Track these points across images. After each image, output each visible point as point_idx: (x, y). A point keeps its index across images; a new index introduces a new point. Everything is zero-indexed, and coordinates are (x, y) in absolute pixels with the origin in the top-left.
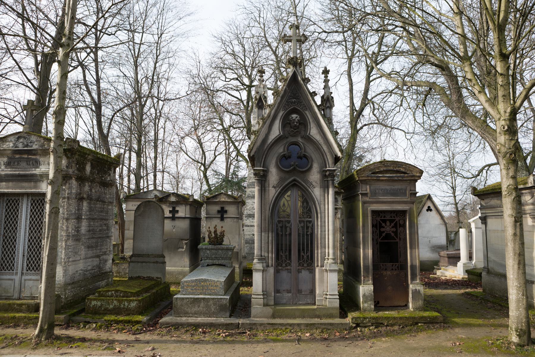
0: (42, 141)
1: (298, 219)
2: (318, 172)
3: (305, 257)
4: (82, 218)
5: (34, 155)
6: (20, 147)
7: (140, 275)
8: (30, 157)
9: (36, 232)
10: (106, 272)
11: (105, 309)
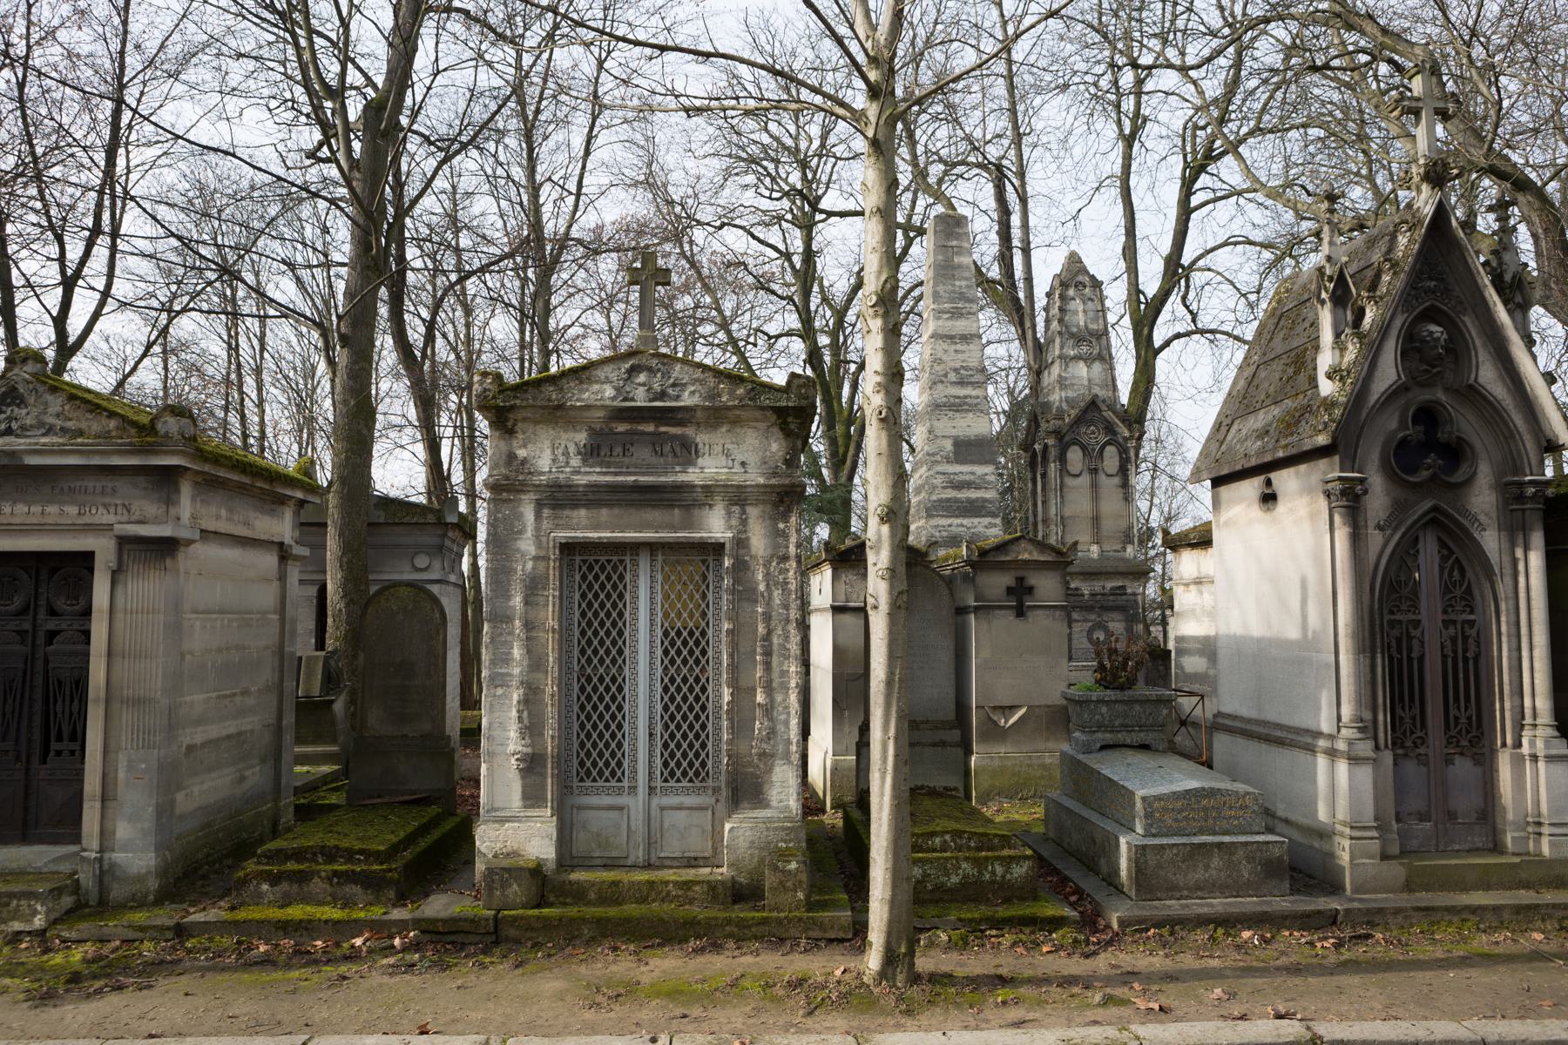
0: (712, 382)
1: (1440, 617)
2: (1491, 487)
3: (1463, 720)
5: (682, 423)
6: (640, 399)
8: (663, 429)
9: (685, 662)
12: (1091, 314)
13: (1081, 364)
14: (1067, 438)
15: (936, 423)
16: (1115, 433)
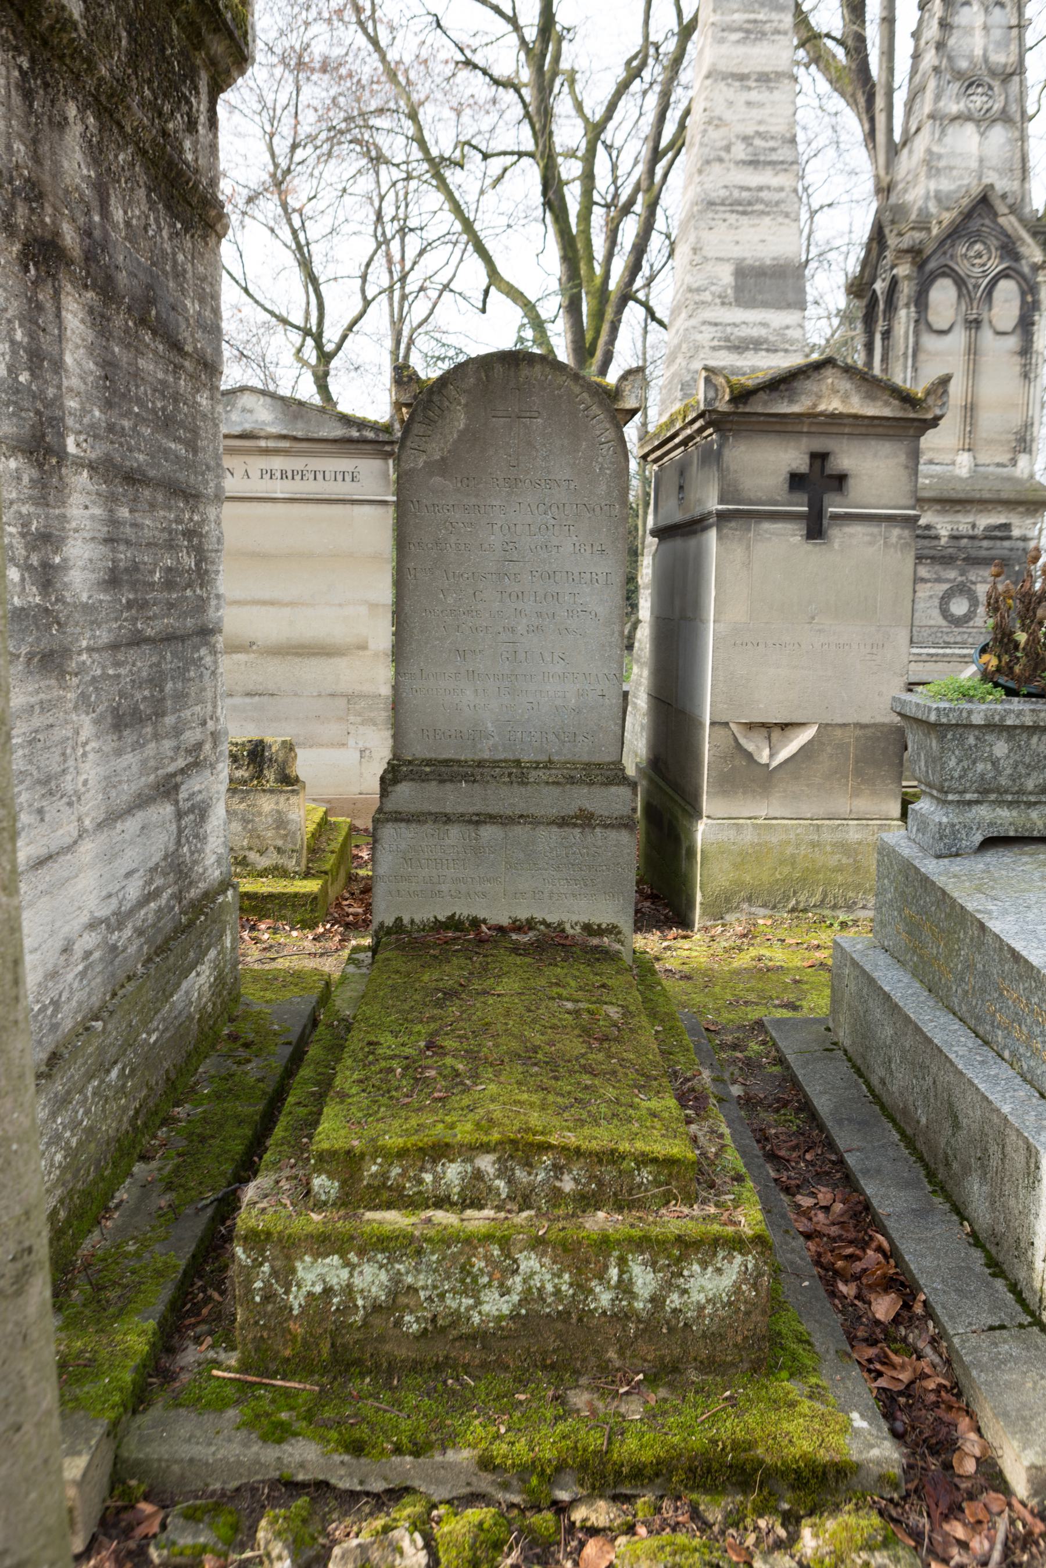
4: (62, 455)
7: (464, 910)
10: (206, 895)
11: (436, 1330)
12: (997, 34)
13: (970, 128)
14: (932, 265)
15: (706, 235)
16: (1016, 257)
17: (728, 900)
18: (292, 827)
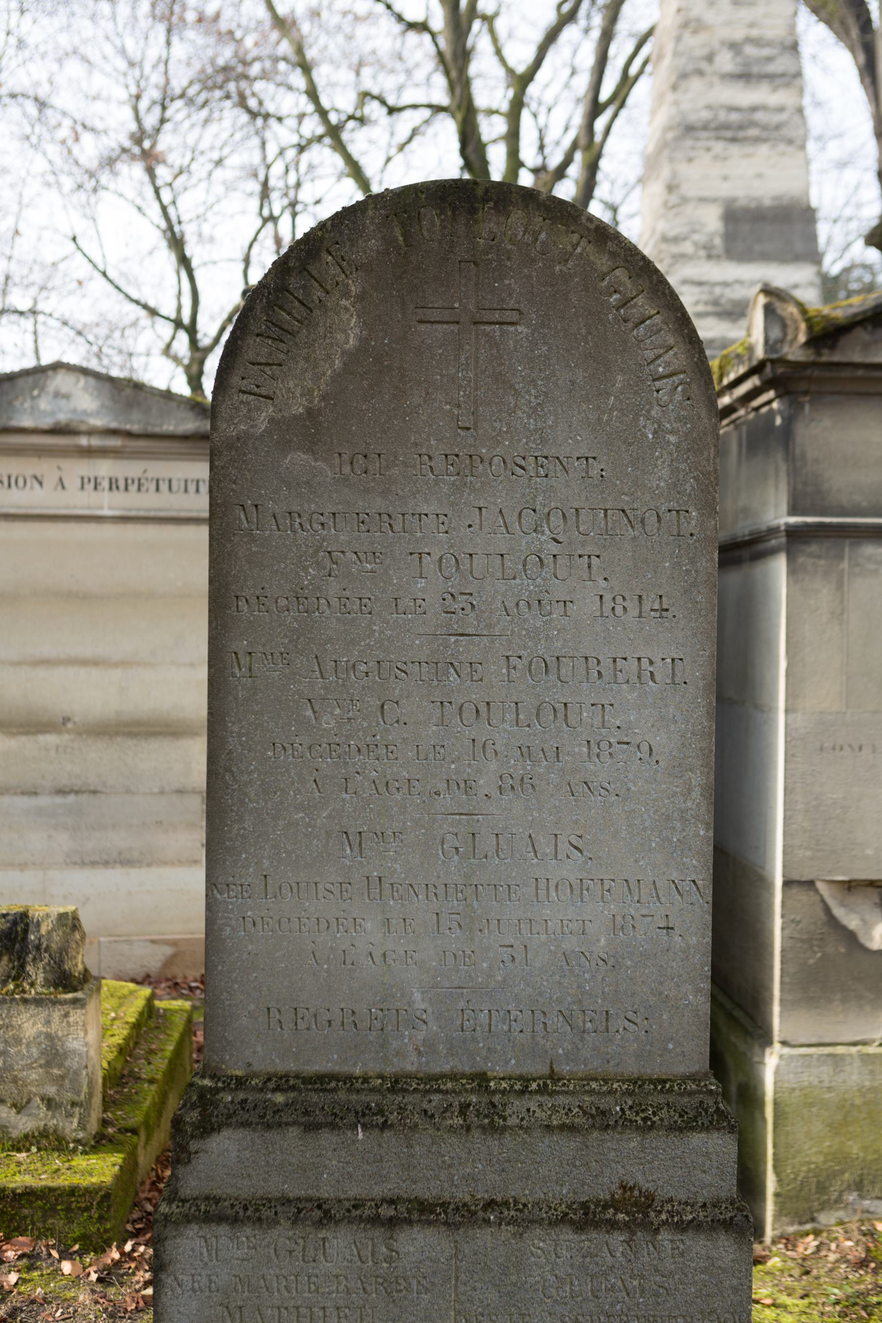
15: (684, 169)
17: (822, 1188)
18: (73, 1063)
